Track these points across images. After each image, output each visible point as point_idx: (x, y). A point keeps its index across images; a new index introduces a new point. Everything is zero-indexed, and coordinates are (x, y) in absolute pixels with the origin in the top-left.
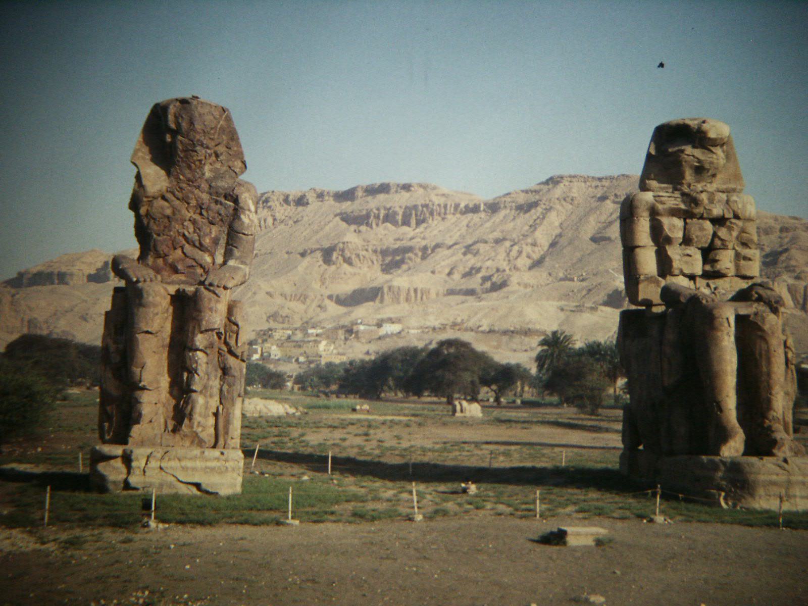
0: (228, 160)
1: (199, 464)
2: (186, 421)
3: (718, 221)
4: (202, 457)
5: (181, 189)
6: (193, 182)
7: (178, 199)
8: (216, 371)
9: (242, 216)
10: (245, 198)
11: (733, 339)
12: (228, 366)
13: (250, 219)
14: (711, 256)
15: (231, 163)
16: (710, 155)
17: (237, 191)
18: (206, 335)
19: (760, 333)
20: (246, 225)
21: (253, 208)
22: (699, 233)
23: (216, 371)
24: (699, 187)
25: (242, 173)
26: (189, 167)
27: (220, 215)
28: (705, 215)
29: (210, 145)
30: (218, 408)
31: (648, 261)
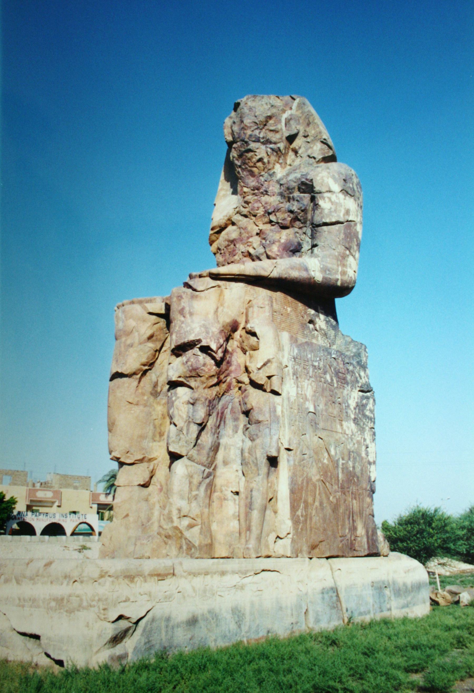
0: (307, 150)
5: (247, 203)
6: (258, 189)
7: (246, 216)
8: (236, 419)
9: (321, 203)
10: (322, 177)
12: (249, 407)
13: (332, 203)
15: (309, 152)
20: (326, 211)
21: (336, 188)
23: (236, 419)
26: (252, 174)
27: (291, 212)
29: (274, 140)
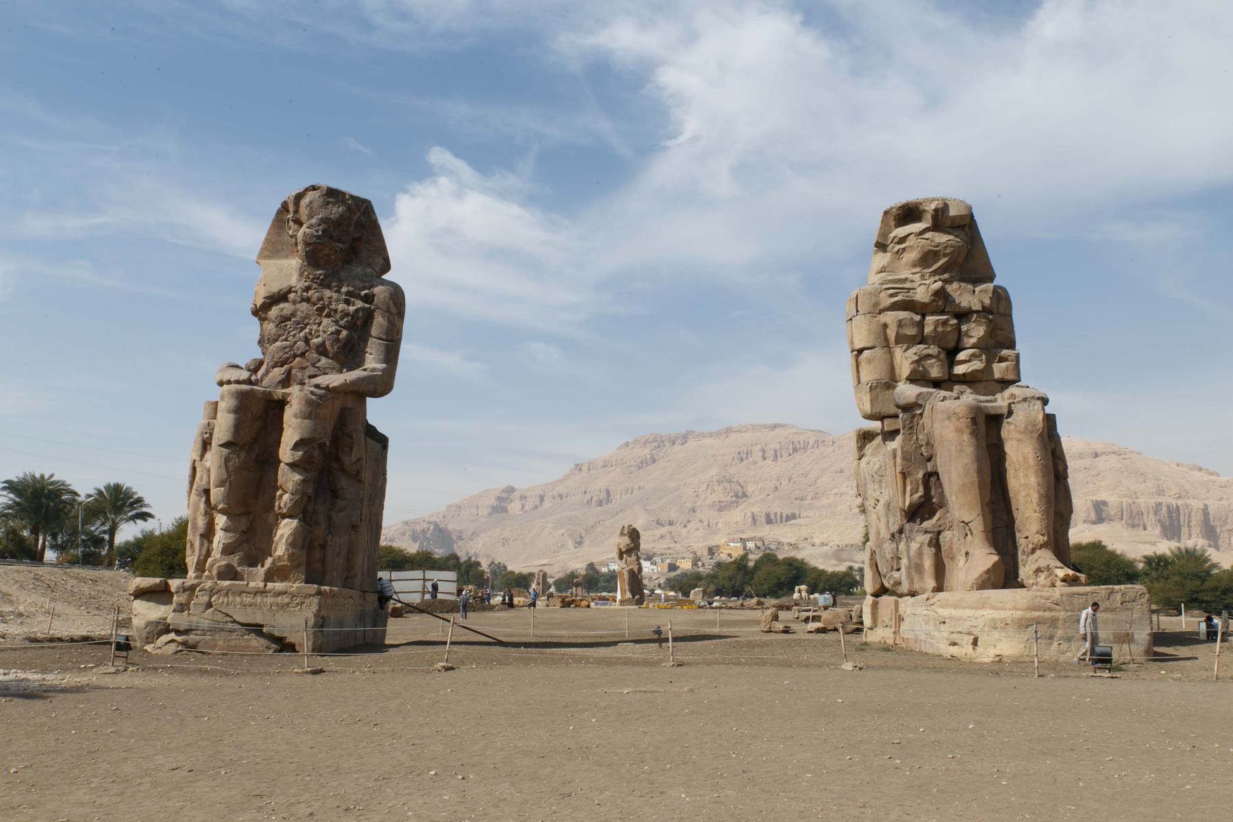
1: (259, 599)
11: (984, 444)
14: (962, 356)
24: (937, 278)
30: (326, 540)
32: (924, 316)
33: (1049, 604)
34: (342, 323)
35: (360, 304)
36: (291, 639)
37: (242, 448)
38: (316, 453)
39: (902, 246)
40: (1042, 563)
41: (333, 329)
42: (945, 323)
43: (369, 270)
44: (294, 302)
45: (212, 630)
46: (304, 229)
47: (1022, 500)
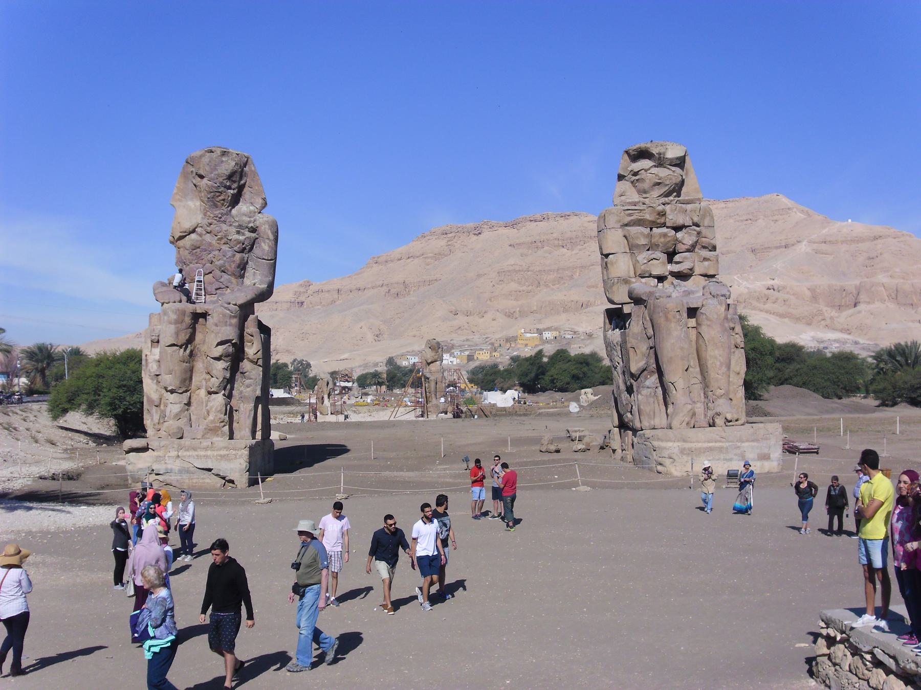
1: (209, 453)
2: (211, 418)
3: (677, 229)
4: (212, 447)
9: (263, 244)
14: (677, 258)
16: (671, 173)
17: (257, 223)
18: (224, 347)
19: (709, 323)
21: (271, 237)
22: (662, 240)
25: (264, 207)
28: (668, 224)
29: (233, 187)
31: (622, 265)
32: (651, 229)
33: (718, 438)
34: (236, 248)
35: (248, 234)
36: (230, 477)
37: (181, 347)
38: (231, 349)
39: (637, 178)
40: (718, 410)
41: (230, 254)
42: (665, 235)
43: (252, 208)
44: (200, 235)
45: (180, 472)
46: (205, 180)
47: (709, 366)
